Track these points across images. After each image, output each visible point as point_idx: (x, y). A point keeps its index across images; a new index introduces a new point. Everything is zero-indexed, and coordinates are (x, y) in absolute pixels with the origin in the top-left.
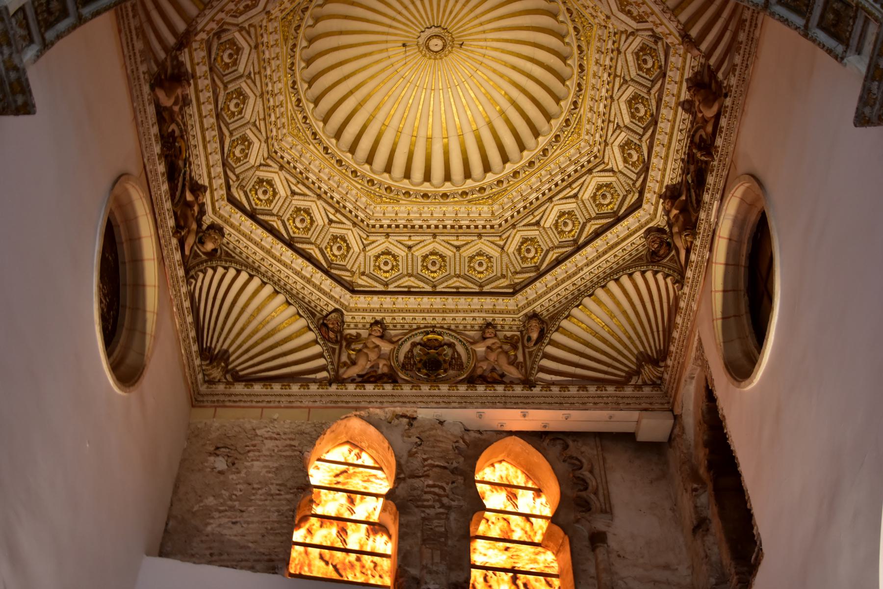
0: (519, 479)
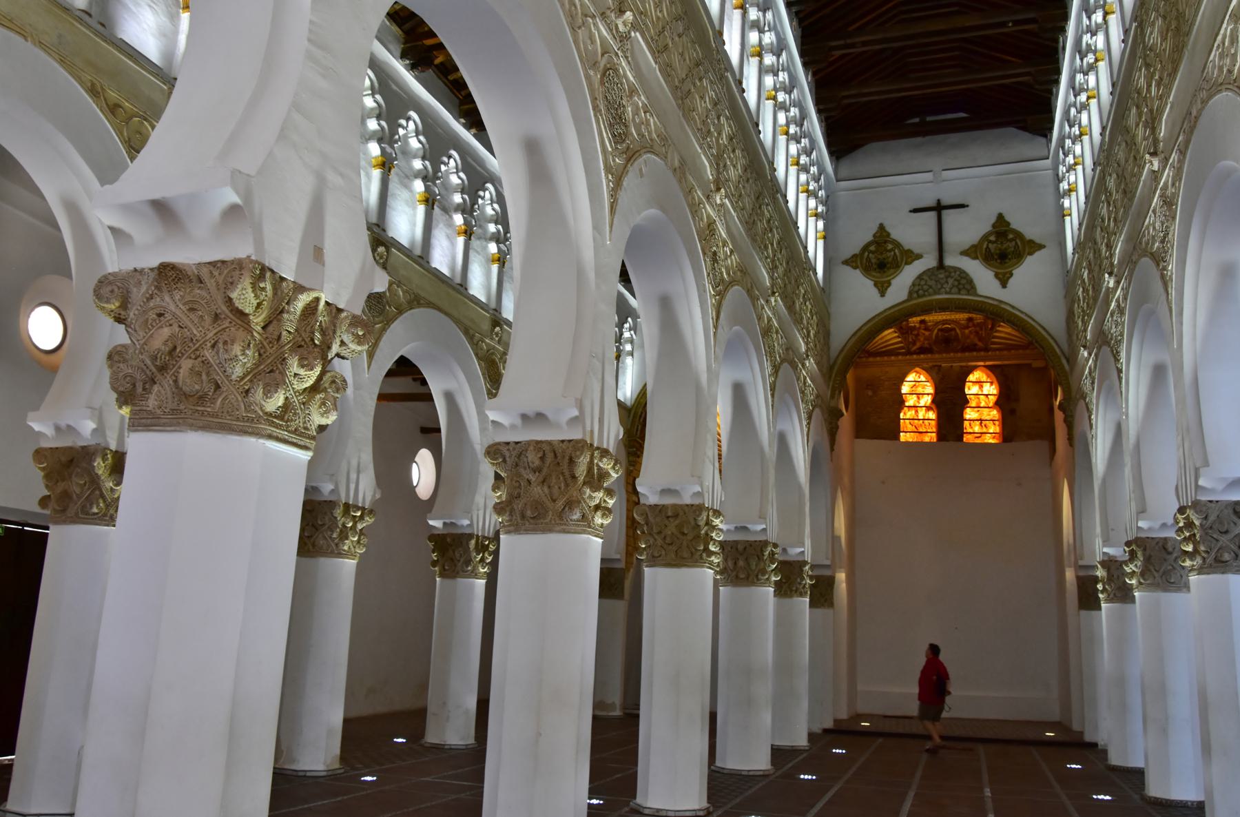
0: (984, 378)
